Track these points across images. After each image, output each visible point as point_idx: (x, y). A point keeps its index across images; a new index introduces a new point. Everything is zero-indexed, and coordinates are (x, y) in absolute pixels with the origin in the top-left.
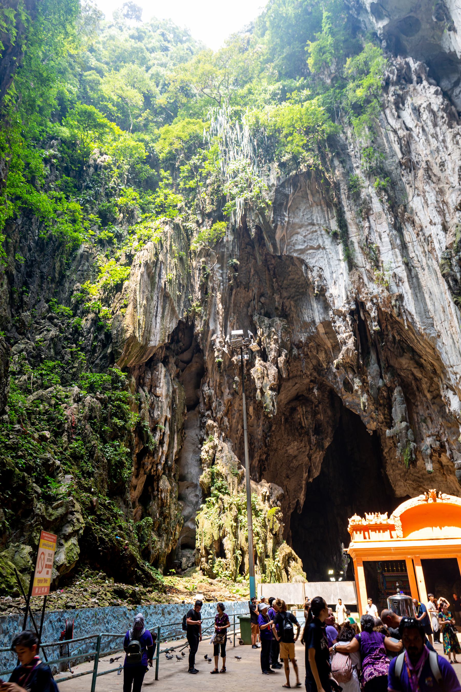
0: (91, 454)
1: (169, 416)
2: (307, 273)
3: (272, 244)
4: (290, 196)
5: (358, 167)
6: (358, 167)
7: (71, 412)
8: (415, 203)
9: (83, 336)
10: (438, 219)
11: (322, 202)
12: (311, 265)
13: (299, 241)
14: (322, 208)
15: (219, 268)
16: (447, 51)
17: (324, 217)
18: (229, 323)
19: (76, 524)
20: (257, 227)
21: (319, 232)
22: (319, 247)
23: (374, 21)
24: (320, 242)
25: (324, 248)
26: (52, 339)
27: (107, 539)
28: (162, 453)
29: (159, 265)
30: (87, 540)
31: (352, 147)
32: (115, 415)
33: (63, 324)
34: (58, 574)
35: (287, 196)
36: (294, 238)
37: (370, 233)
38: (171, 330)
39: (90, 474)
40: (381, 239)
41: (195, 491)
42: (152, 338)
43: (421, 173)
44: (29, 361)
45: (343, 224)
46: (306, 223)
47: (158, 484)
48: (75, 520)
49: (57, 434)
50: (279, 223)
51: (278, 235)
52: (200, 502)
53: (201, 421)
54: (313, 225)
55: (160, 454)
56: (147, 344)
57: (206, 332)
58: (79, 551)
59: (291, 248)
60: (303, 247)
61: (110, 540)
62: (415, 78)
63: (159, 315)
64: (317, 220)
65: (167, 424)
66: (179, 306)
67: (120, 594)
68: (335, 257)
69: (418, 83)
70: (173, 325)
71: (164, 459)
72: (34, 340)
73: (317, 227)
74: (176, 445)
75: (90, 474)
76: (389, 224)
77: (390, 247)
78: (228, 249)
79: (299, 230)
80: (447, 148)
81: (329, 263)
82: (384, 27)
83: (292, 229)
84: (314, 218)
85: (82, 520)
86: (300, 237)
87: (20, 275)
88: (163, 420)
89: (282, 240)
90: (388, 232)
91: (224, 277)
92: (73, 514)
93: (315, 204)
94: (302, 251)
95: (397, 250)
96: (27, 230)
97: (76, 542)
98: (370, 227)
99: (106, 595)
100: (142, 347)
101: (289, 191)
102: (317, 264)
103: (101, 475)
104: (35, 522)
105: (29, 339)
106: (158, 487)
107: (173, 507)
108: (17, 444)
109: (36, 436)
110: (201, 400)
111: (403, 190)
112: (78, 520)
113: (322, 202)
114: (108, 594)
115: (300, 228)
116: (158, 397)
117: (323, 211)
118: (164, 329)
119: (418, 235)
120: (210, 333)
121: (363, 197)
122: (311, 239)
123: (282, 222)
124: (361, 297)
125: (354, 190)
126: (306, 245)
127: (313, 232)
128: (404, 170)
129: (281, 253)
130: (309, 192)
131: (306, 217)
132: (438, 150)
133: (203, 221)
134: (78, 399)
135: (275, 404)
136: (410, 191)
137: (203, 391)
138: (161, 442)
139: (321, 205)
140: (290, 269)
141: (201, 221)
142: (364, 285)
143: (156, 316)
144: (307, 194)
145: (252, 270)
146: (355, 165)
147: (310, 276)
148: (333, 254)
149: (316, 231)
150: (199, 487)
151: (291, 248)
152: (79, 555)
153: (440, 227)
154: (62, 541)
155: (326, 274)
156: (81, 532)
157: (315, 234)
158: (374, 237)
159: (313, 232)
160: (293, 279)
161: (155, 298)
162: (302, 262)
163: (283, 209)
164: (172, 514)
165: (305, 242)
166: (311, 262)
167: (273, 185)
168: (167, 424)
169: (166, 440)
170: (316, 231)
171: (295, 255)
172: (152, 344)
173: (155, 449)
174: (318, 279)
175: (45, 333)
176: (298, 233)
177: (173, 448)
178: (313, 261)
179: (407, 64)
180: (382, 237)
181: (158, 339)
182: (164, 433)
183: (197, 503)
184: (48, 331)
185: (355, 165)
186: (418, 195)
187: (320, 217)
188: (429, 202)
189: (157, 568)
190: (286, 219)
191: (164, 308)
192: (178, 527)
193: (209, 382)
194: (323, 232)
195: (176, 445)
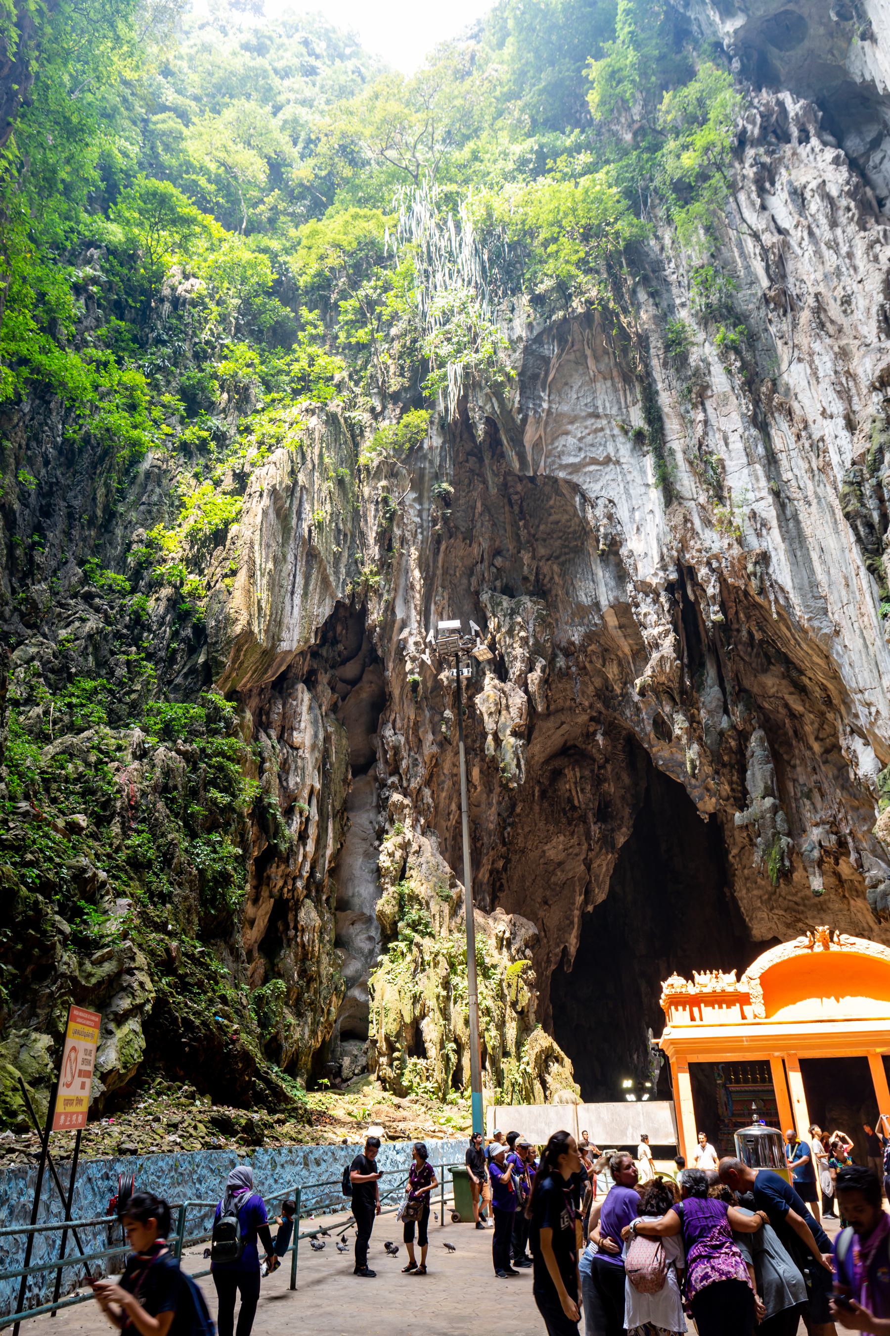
0: (167, 859)
1: (318, 786)
2: (584, 511)
3: (517, 454)
4: (553, 361)
5: (683, 305)
6: (683, 305)
7: (127, 777)
8: (794, 376)
9: (150, 631)
10: (838, 407)
11: (615, 373)
12: (592, 496)
13: (570, 447)
14: (613, 385)
15: (414, 500)
16: (859, 80)
17: (619, 402)
18: (433, 607)
19: (139, 993)
20: (489, 421)
21: (608, 432)
22: (608, 460)
23: (717, 19)
24: (611, 450)
25: (618, 462)
26: (90, 637)
27: (198, 1022)
28: (305, 856)
29: (298, 494)
30: (159, 1023)
31: (672, 265)
32: (213, 783)
33: (112, 608)
34: (103, 1088)
35: (546, 360)
36: (560, 443)
37: (706, 434)
38: (322, 620)
39: (165, 898)
40: (727, 444)
41: (368, 929)
42: (285, 635)
43: (805, 316)
44: (46, 679)
46: (583, 414)
47: (296, 916)
48: (136, 985)
49: (101, 821)
50: (531, 413)
51: (530, 436)
52: (377, 950)
53: (379, 796)
54: (597, 416)
55: (300, 859)
56: (274, 647)
57: (389, 624)
58: (143, 1044)
59: (554, 462)
60: (577, 460)
61: (204, 1023)
62: (795, 132)
63: (299, 591)
64: (604, 408)
65: (314, 801)
66: (337, 573)
67: (223, 1126)
68: (639, 481)
69: (800, 143)
70: (326, 610)
71: (307, 868)
72: (55, 639)
73: (604, 422)
74: (330, 842)
75: (165, 898)
76: (743, 415)
77: (745, 460)
78: (431, 462)
79: (569, 427)
80: (855, 269)
81: (627, 490)
82: (736, 32)
83: (556, 425)
84: (599, 403)
85: (149, 986)
86: (571, 441)
87: (27, 512)
88: (306, 793)
89: (537, 445)
90: (741, 431)
91: (425, 517)
92: (133, 975)
93: (600, 377)
94: (575, 468)
95: (757, 466)
96: (41, 424)
97: (138, 1028)
98: (706, 422)
99: (195, 1128)
100: (265, 653)
101: (551, 350)
102: (603, 493)
103: (186, 898)
104: (59, 989)
105: (45, 636)
106: (296, 922)
107: (325, 959)
108: (23, 840)
109: (60, 823)
110: (380, 754)
111: (771, 351)
112: (142, 984)
113: (615, 373)
114: (200, 1125)
115: (572, 423)
116: (297, 749)
117: (616, 390)
118: (307, 617)
119: (799, 437)
120: (397, 626)
121: (693, 364)
122: (592, 445)
123: (536, 412)
124: (687, 556)
125: (676, 349)
127: (597, 431)
128: (773, 310)
129: (535, 472)
130: (588, 352)
131: (583, 402)
132: (838, 273)
133: (384, 408)
134: (142, 754)
135: (522, 762)
136: (784, 352)
137: (383, 737)
138: (303, 836)
139: (612, 378)
140: (552, 502)
141: (379, 409)
142: (695, 534)
143: (292, 593)
144: (586, 357)
145: (479, 505)
146: (678, 301)
147: (590, 516)
148: (635, 473)
149: (602, 429)
150: (375, 923)
151: (554, 462)
152: (144, 1052)
153: (841, 422)
154: (112, 1026)
155: (622, 513)
156: (148, 1007)
157: (601, 434)
158: (714, 442)
159: (597, 431)
160: (557, 523)
161: (290, 558)
162: (576, 488)
163: (539, 386)
164: (324, 973)
165: (580, 449)
166: (593, 489)
167: (520, 338)
168: (314, 801)
169: (312, 831)
170: (602, 429)
171: (562, 475)
172: (285, 646)
173: (291, 849)
174: (605, 521)
175: (77, 624)
176: (567, 433)
177: (325, 847)
178: (596, 487)
179: (781, 104)
180: (730, 440)
181: (296, 637)
182: (308, 819)
183: (371, 952)
184: (83, 620)
185: (678, 301)
186: (800, 360)
187: (611, 402)
188: (821, 374)
189: (294, 1076)
190: (545, 405)
191: (307, 578)
192: (334, 999)
193: (394, 721)
194: (616, 431)
195: (330, 842)
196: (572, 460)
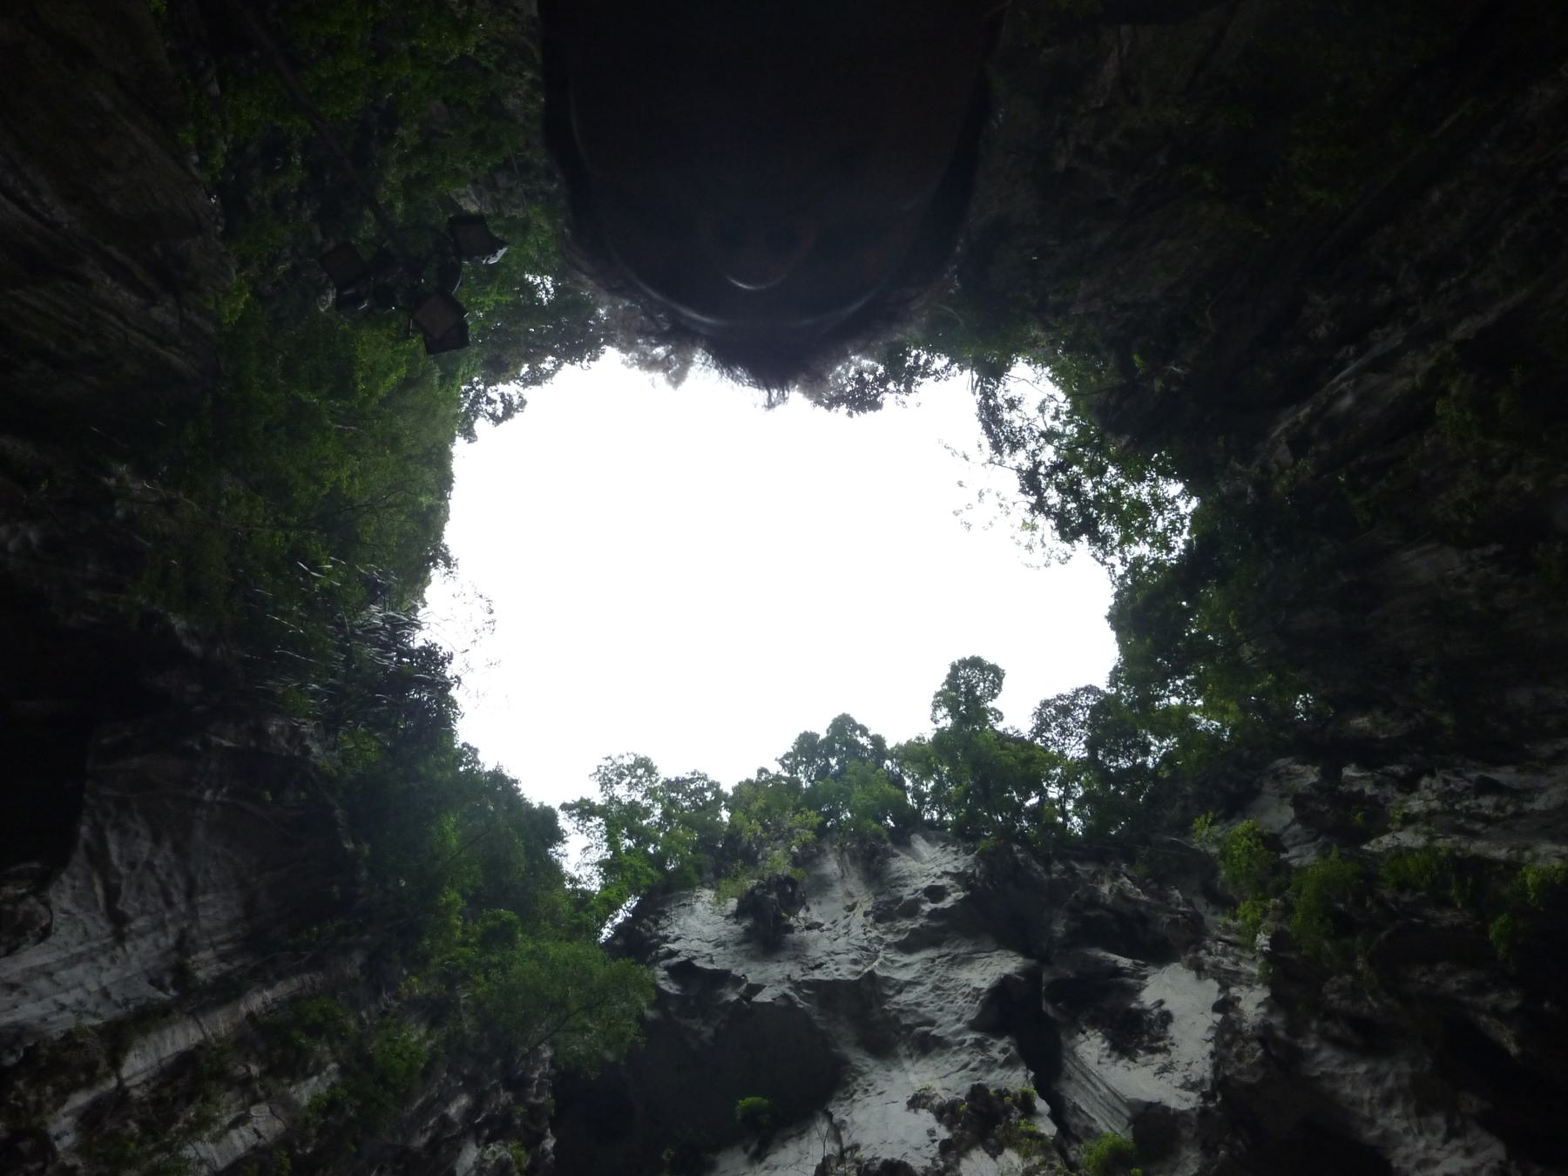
12: (51, 894)
21: (168, 916)
22: (118, 921)
24: (140, 923)
25: (120, 938)
45: (227, 990)
54: (189, 895)
60: (115, 860)
79: (168, 845)
81: (77, 959)
84: (210, 897)
86: (145, 846)
94: (98, 858)
115: (177, 848)
122: (141, 888)
124: (20, 1084)
126: (123, 870)
146: (364, 1014)
157: (161, 903)
158: (227, 1106)
165: (132, 866)
166: (62, 898)
170: (170, 904)
171: (84, 830)
176: (156, 840)
178: (66, 903)
196: (114, 849)
